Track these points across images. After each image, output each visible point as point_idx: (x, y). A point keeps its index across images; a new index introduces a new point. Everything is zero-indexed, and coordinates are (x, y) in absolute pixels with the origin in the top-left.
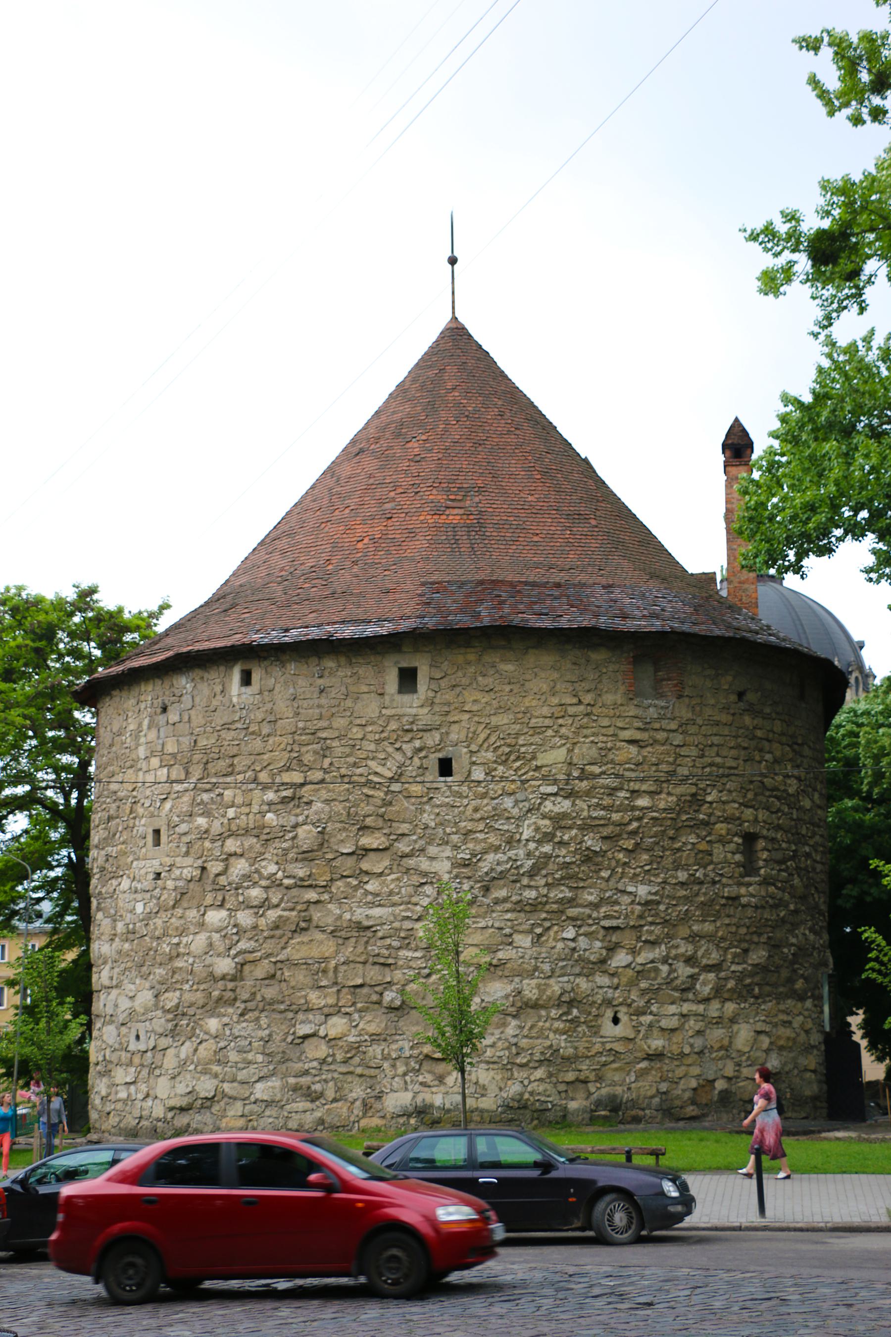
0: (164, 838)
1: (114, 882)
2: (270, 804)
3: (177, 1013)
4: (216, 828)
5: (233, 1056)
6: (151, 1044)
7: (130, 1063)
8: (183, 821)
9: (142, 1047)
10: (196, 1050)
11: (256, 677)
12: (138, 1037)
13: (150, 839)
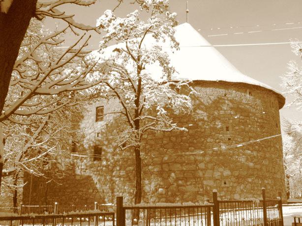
0: (230, 129)
1: (203, 139)
2: (258, 126)
3: (238, 177)
4: (247, 129)
5: (256, 188)
6: (231, 184)
7: (223, 191)
8: (237, 126)
9: (226, 185)
10: (245, 187)
11: (253, 94)
12: (225, 183)
13: (225, 129)
